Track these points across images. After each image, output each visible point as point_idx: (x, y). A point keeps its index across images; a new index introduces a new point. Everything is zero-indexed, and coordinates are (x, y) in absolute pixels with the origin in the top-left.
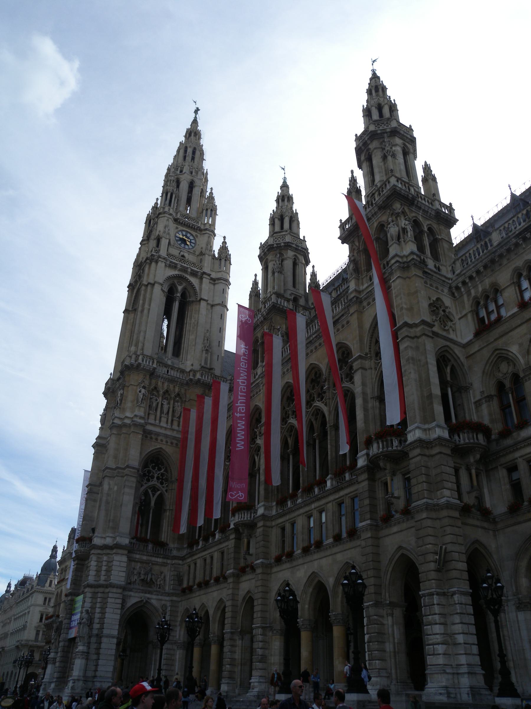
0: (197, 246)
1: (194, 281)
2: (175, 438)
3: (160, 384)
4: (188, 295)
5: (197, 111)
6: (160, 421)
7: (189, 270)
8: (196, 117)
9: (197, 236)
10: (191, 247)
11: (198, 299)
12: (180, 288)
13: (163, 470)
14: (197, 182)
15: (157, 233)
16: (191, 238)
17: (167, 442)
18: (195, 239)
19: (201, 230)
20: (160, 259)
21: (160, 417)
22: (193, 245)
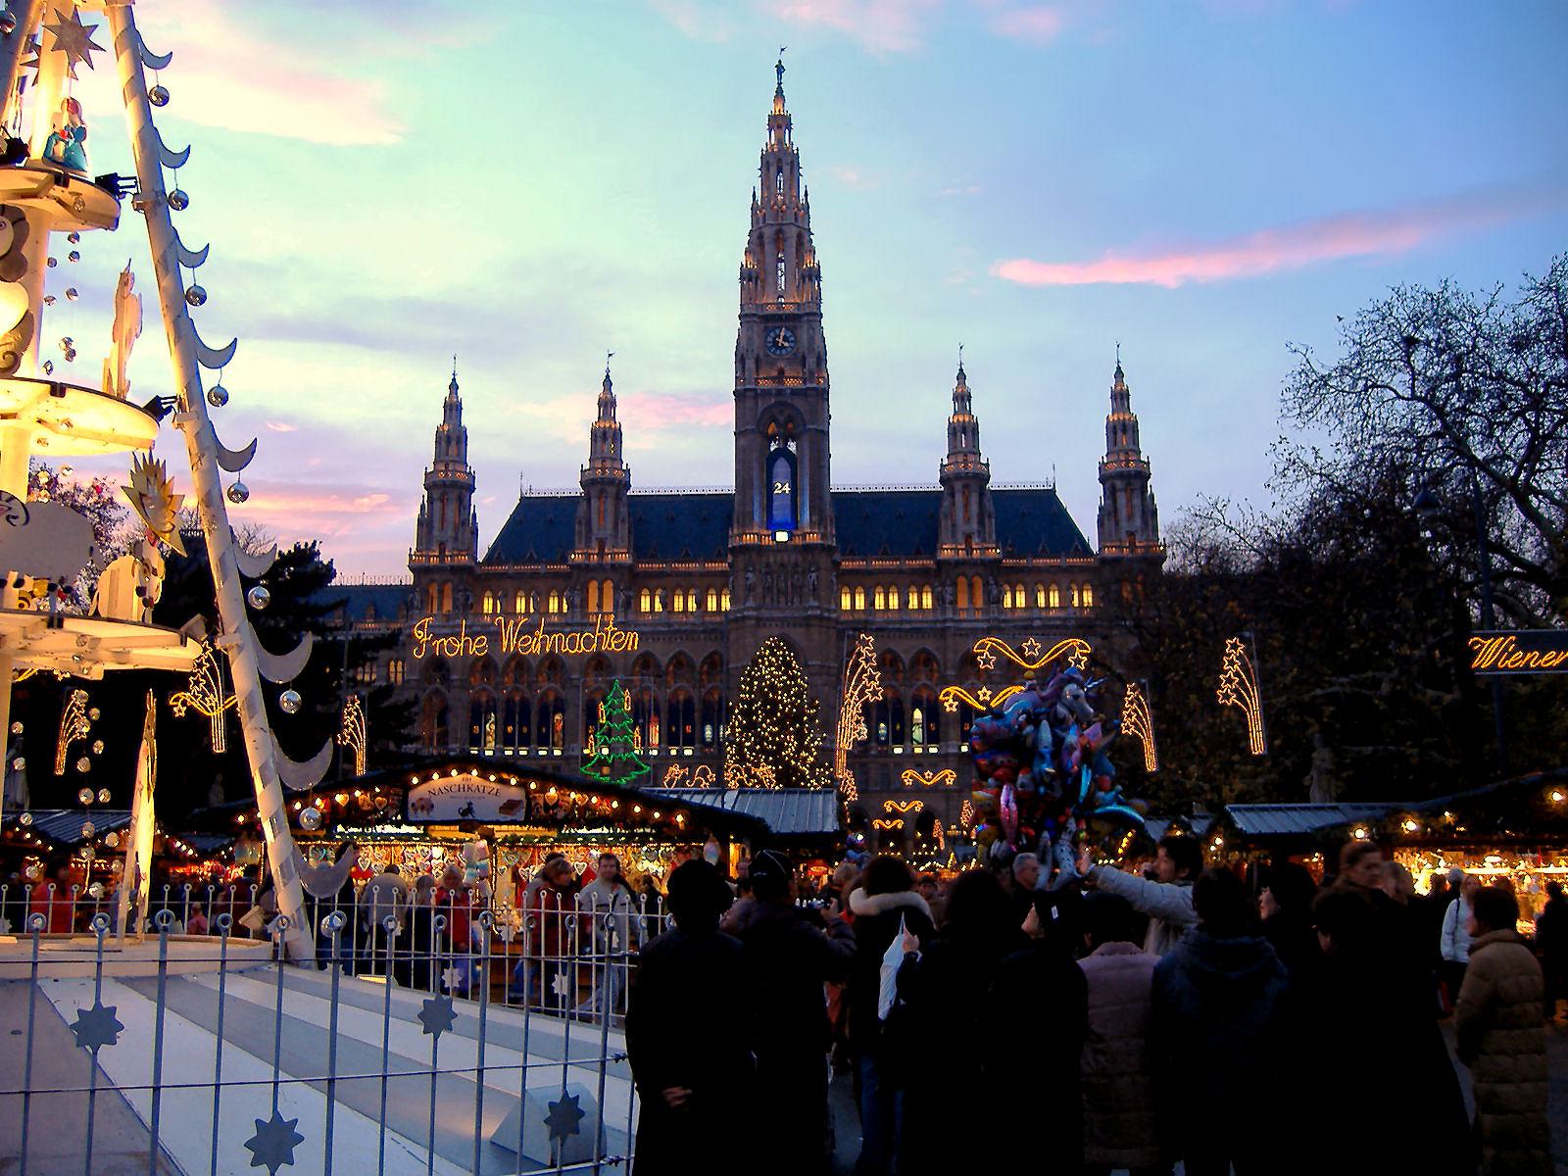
1: (799, 403)
3: (771, 560)
5: (780, 69)
8: (780, 84)
18: (794, 334)
19: (800, 316)
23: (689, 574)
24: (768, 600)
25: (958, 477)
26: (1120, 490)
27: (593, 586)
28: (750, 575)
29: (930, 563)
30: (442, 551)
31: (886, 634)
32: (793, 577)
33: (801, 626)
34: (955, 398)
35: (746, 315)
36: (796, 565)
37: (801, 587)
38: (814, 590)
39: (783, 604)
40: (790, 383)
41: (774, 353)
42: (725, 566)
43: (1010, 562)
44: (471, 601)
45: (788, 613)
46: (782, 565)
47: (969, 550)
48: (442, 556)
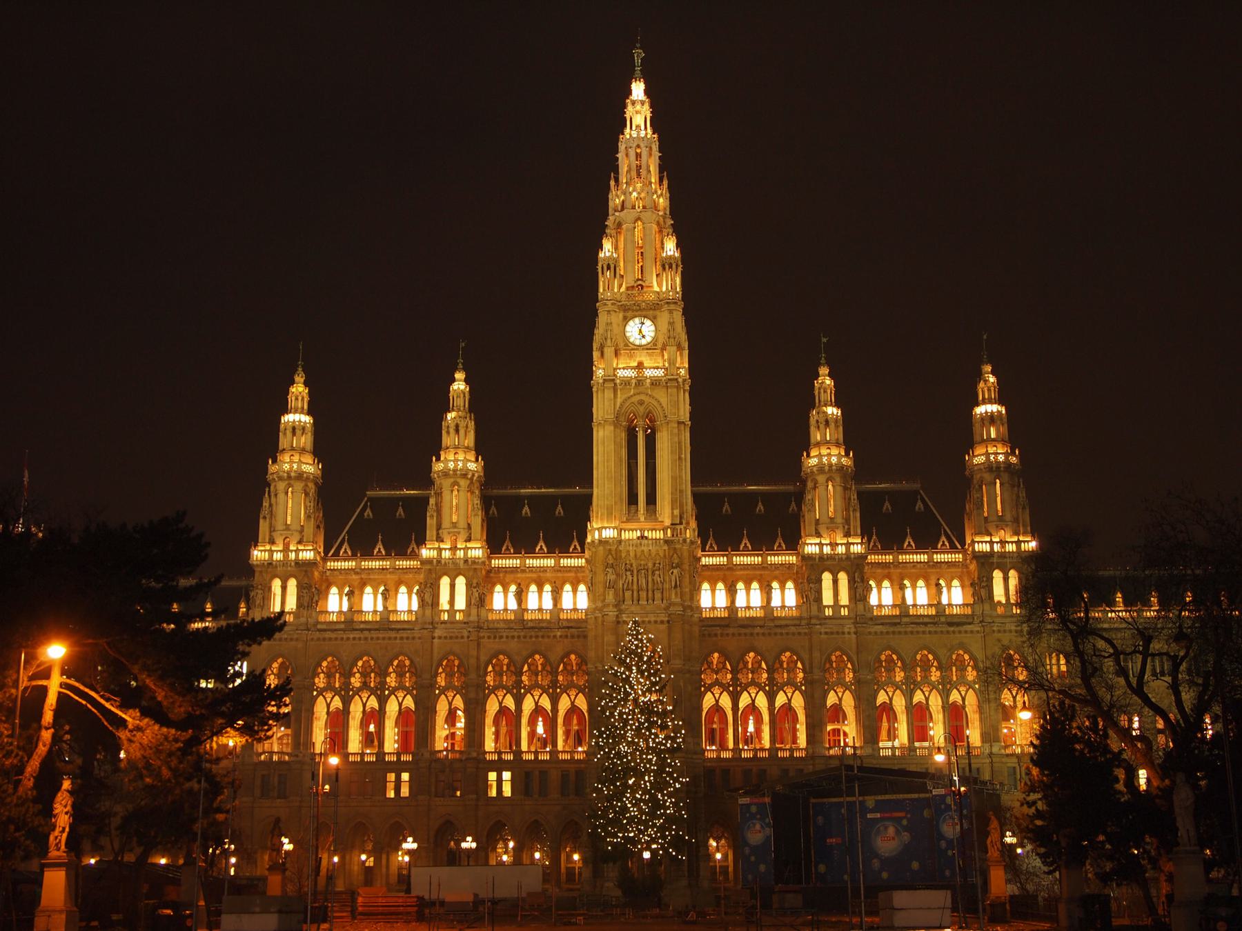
3: (632, 554)
12: (642, 409)
23: (543, 569)
24: (628, 594)
27: (445, 582)
28: (610, 570)
29: (792, 559)
30: (286, 550)
31: (747, 631)
32: (653, 574)
40: (648, 373)
42: (581, 562)
43: (872, 558)
44: (316, 598)
45: (648, 608)
47: (833, 545)
48: (286, 550)
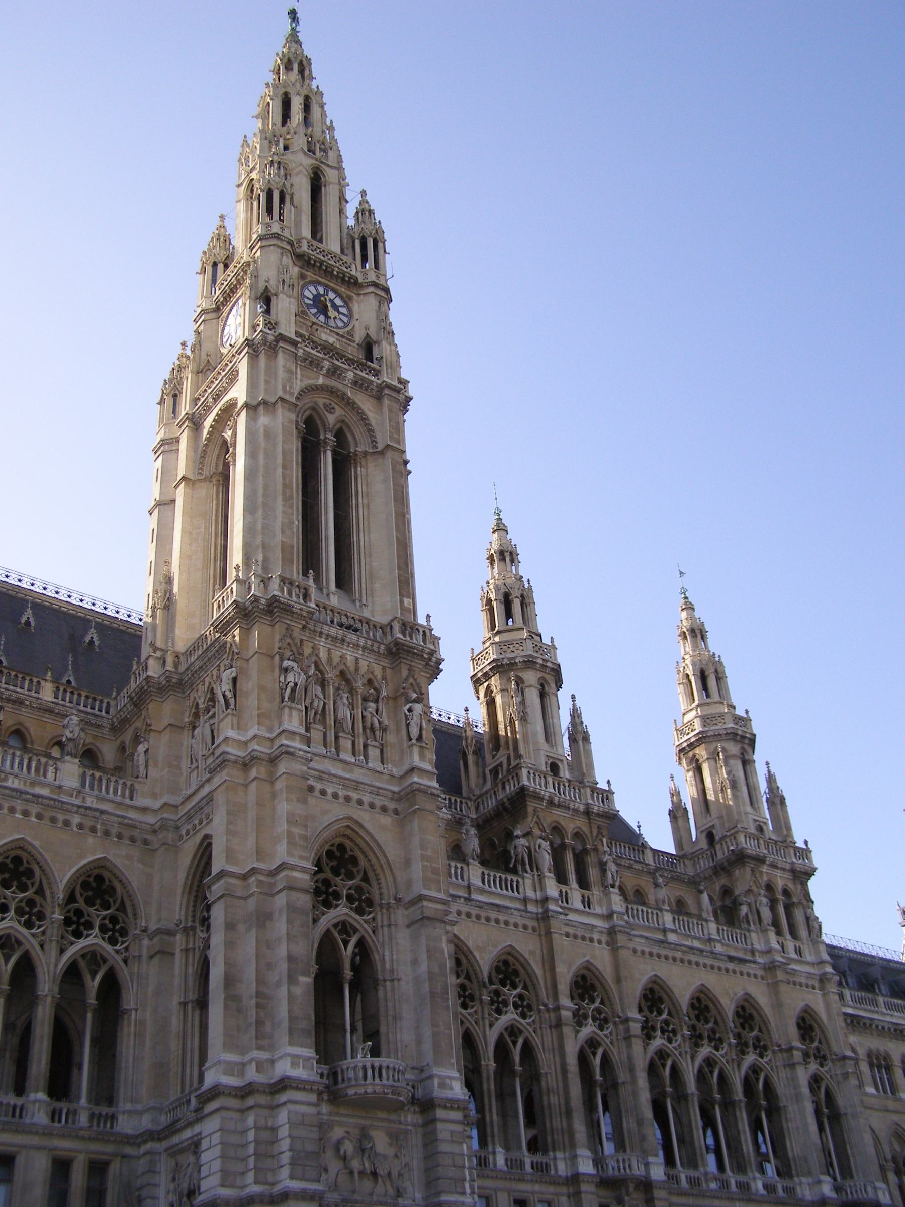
0: (354, 322)
1: (366, 404)
2: (377, 791)
3: (323, 655)
4: (350, 438)
6: (337, 749)
7: (350, 375)
9: (350, 298)
10: (340, 324)
11: (380, 446)
12: (331, 419)
13: (359, 877)
14: (330, 175)
15: (262, 285)
16: (338, 302)
17: (360, 802)
18: (346, 305)
20: (281, 344)
21: (337, 738)
22: (346, 320)
24: (316, 734)
25: (529, 663)
26: (734, 757)
33: (384, 809)
34: (491, 559)
35: (277, 236)
36: (370, 682)
37: (384, 729)
38: (420, 738)
39: (346, 756)
41: (314, 315)
45: (358, 774)
46: (342, 673)
